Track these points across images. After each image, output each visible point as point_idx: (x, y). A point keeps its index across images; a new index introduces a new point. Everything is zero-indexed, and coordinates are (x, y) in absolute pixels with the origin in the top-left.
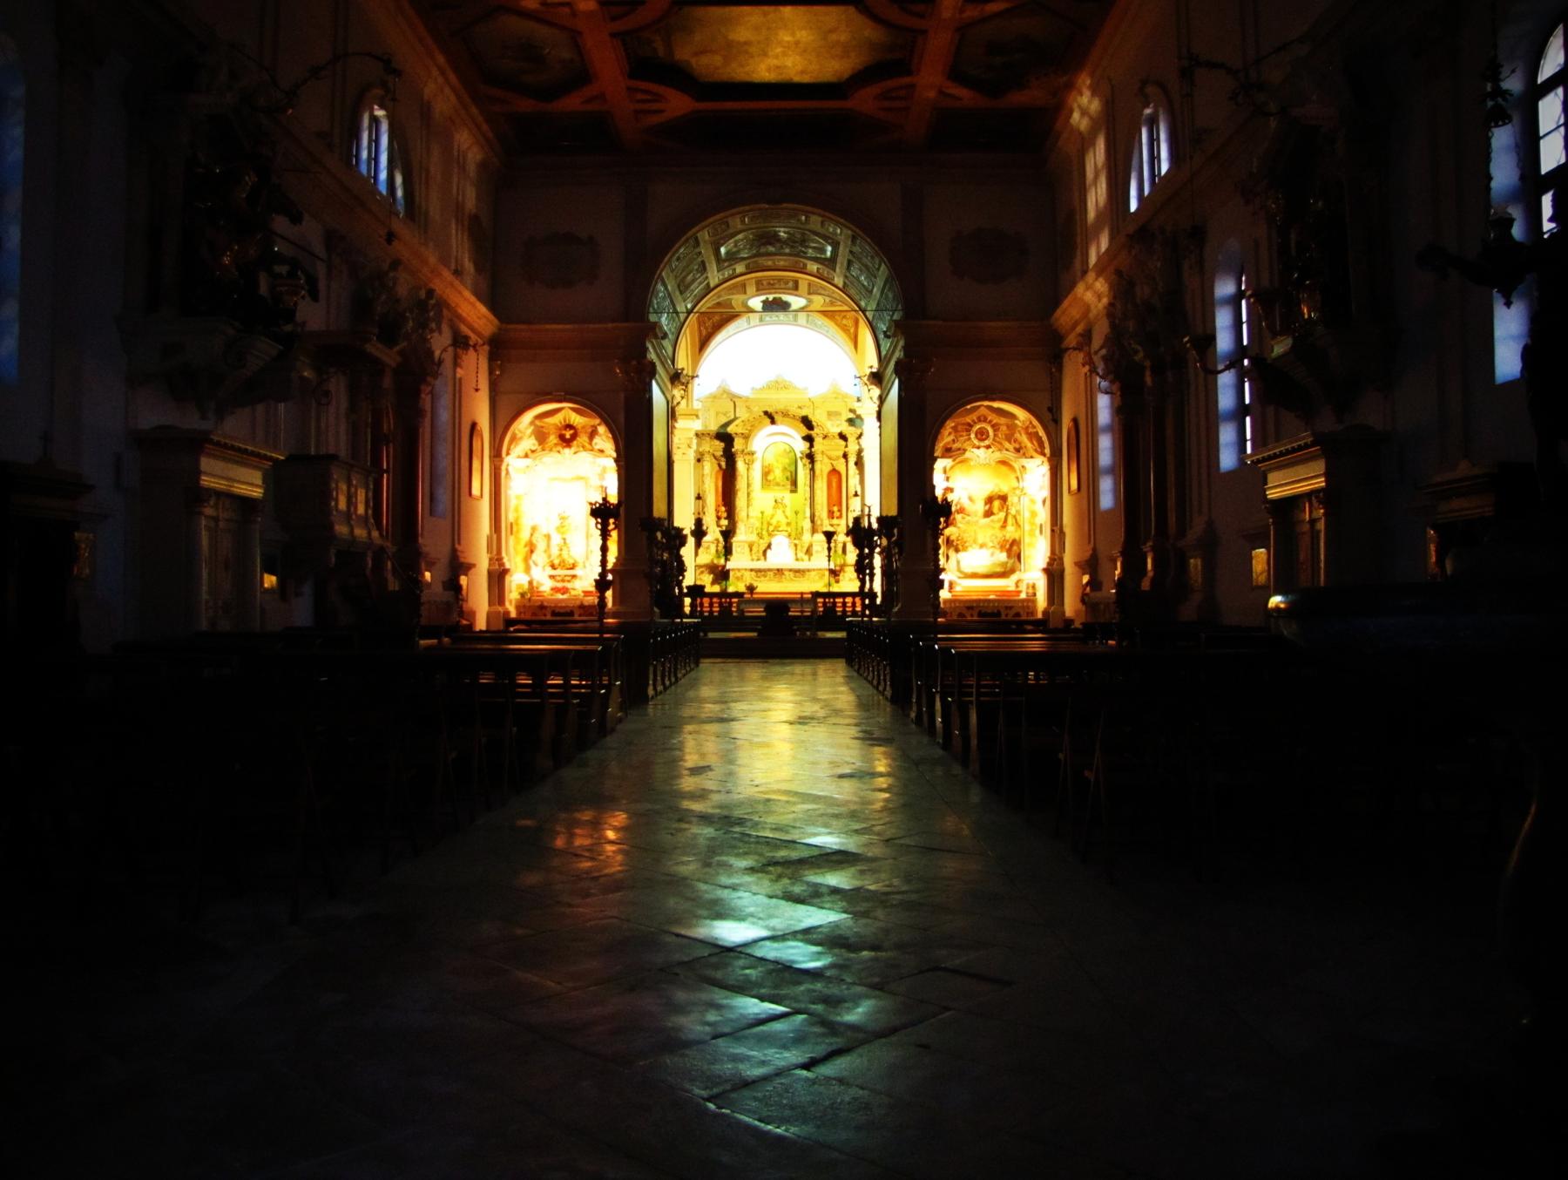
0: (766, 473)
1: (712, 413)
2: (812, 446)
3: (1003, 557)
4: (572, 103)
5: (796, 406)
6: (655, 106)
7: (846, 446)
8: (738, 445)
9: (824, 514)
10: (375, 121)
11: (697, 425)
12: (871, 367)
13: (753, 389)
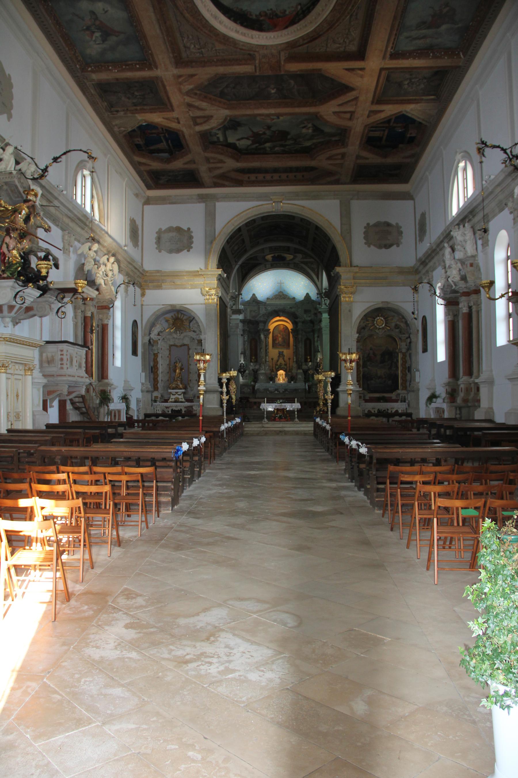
0: (274, 340)
1: (248, 310)
2: (297, 327)
3: (390, 382)
4: (178, 164)
5: (289, 307)
6: (219, 165)
7: (314, 327)
8: (261, 326)
9: (303, 360)
10: (84, 176)
11: (241, 317)
12: (325, 289)
13: (268, 299)
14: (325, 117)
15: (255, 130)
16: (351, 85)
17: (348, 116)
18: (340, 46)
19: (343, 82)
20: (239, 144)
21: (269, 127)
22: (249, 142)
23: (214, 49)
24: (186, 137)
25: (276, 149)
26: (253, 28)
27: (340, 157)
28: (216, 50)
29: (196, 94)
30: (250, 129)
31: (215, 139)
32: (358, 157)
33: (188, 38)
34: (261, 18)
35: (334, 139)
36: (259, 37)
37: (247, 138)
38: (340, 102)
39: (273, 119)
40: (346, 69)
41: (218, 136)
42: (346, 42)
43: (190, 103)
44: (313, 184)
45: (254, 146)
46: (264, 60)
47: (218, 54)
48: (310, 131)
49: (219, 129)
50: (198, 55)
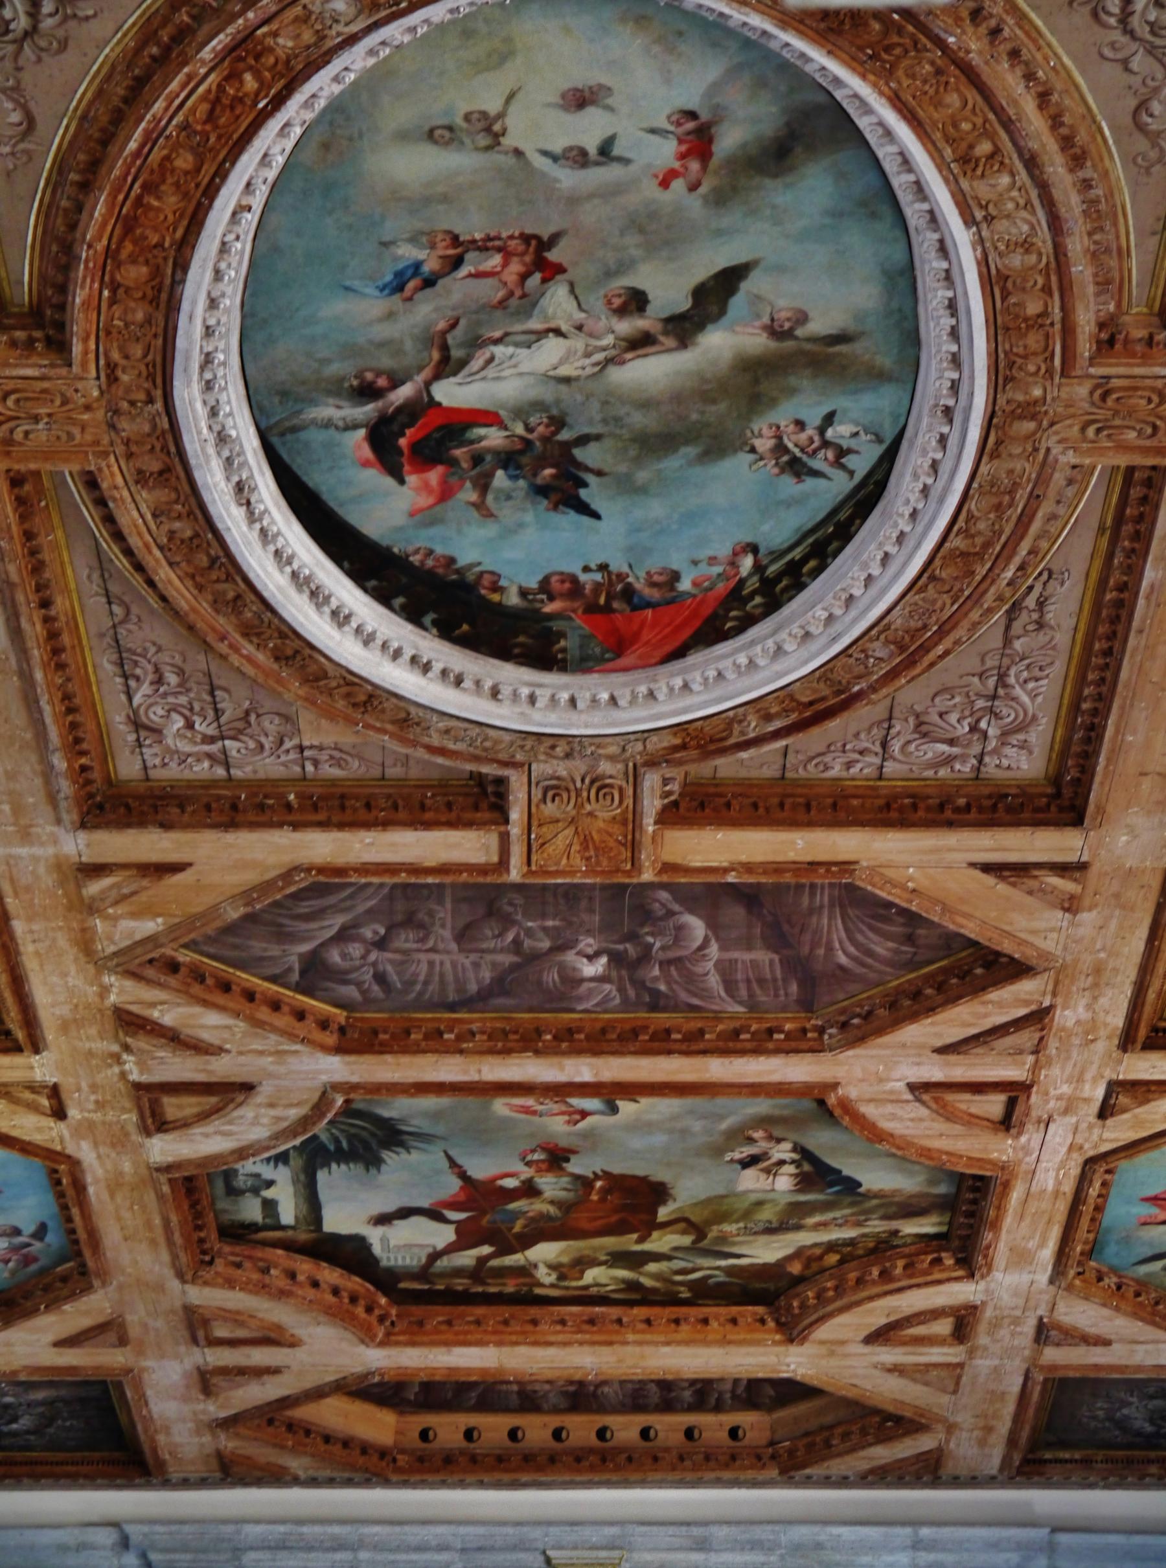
6: (259, 1356)
14: (869, 1111)
15: (480, 1168)
16: (1007, 947)
17: (994, 1105)
18: (955, 750)
19: (970, 930)
20: (384, 1240)
21: (557, 1158)
22: (443, 1235)
23: (288, 744)
24: (91, 1190)
25: (592, 1275)
26: (503, 652)
27: (943, 1327)
28: (301, 748)
29: (173, 967)
30: (453, 1163)
31: (251, 1210)
32: (1043, 1333)
33: (159, 681)
34: (549, 608)
35: (911, 1228)
36: (532, 699)
37: (434, 1214)
38: (955, 1034)
39: (584, 1114)
40: (987, 868)
41: (268, 1194)
42: (985, 735)
43: (134, 1008)
44: (791, 1483)
45: (467, 1258)
46: (550, 809)
47: (309, 768)
48: (784, 1182)
49: (282, 1158)
50: (202, 770)
